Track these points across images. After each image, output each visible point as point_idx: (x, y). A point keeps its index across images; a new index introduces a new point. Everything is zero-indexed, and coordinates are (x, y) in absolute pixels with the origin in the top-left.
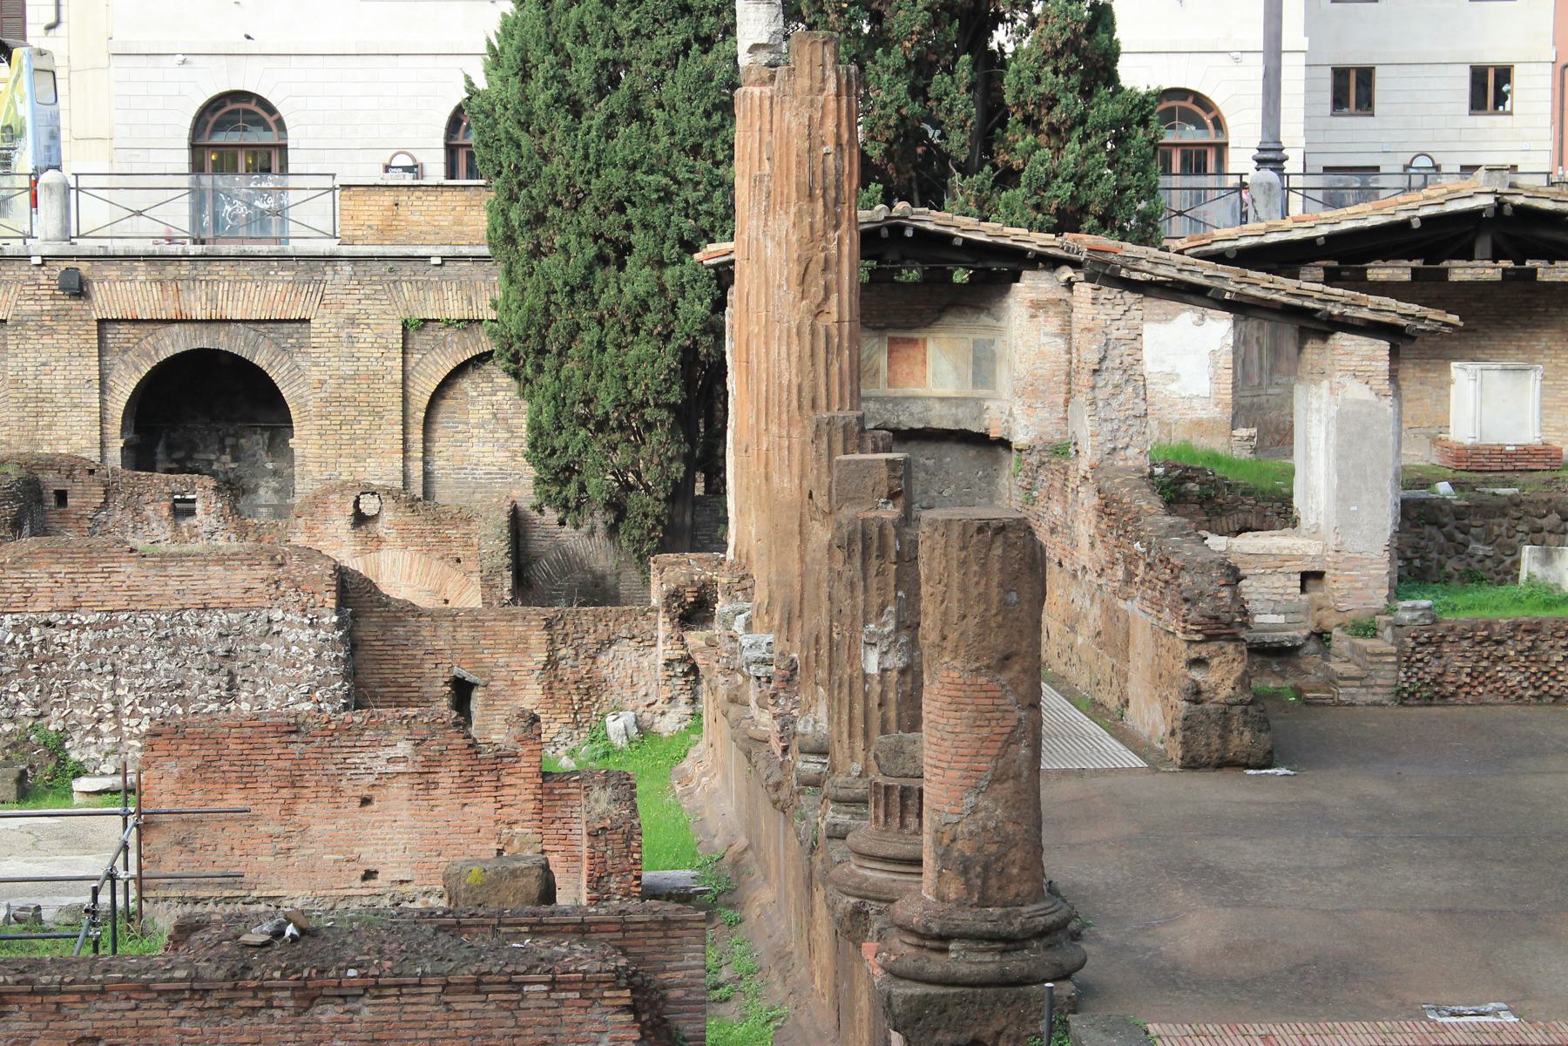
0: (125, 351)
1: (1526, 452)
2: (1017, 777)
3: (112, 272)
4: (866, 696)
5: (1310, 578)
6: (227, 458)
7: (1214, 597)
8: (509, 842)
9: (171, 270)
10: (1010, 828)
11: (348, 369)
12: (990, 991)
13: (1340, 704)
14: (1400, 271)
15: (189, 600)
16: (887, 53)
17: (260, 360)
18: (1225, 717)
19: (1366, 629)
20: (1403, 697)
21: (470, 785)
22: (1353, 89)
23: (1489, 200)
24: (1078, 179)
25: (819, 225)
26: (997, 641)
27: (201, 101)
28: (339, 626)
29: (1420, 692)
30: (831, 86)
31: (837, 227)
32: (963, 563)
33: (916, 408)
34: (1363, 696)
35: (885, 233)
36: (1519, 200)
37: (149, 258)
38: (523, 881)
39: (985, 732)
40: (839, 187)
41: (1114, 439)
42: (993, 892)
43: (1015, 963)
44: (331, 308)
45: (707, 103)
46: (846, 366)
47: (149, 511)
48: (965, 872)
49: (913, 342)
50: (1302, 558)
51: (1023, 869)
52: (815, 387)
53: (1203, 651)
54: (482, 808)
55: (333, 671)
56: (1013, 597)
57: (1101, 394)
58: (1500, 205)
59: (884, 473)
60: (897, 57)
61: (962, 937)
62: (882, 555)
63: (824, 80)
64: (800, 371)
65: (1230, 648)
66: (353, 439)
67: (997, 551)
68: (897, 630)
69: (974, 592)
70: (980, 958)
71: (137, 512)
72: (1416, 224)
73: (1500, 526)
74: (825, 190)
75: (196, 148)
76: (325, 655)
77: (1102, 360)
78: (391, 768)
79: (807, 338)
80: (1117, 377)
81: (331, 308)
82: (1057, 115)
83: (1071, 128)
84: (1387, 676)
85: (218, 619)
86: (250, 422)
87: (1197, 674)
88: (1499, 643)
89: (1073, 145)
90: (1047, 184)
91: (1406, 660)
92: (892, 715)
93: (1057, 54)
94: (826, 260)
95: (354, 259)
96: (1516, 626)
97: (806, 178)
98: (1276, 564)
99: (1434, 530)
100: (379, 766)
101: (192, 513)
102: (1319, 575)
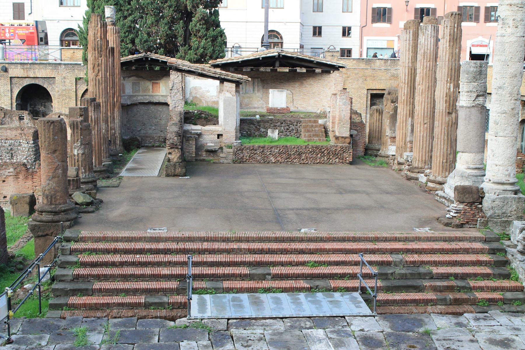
0: (16, 84)
1: (283, 109)
2: (58, 177)
3: (13, 67)
4: (75, 159)
5: (219, 136)
6: (43, 107)
7: (173, 139)
8: (35, 190)
9: (25, 66)
10: (57, 188)
11: (64, 88)
12: (50, 224)
13: (221, 163)
14: (248, 69)
15: (3, 138)
16: (163, 20)
17: (45, 86)
18: (175, 165)
19: (230, 147)
20: (234, 162)
21: (26, 178)
22: (317, 31)
23: (277, 54)
24: (204, 48)
25: (97, 56)
26: (53, 147)
27: (62, 30)
28: (33, 143)
29: (239, 160)
30: (99, 26)
31: (101, 57)
32: (44, 130)
33: (157, 98)
34: (226, 161)
35: (144, 59)
36: (283, 54)
37: (21, 64)
38: (25, 199)
39: (50, 167)
40: (101, 48)
41: (175, 104)
42: (53, 202)
43: (56, 218)
44: (59, 75)
45: (125, 30)
46: (103, 88)
47: (14, 118)
48: (47, 198)
49: (157, 83)
50: (217, 131)
51: (61, 197)
52: (96, 92)
53: (171, 151)
54: (29, 183)
55: (32, 153)
56: (56, 137)
57: (172, 95)
58: (279, 55)
59: (79, 110)
60: (166, 20)
61: (45, 212)
62: (77, 129)
63: (97, 24)
64: (93, 88)
65: (176, 150)
66: (65, 104)
67: (52, 127)
68: (81, 145)
69: (47, 136)
70: (49, 216)
71: (11, 119)
72: (261, 59)
73: (267, 125)
74: (98, 49)
75: (62, 41)
76: (30, 150)
77: (173, 87)
78: (9, 174)
79: (94, 81)
80: (176, 91)
81: (59, 75)
82: (200, 34)
83: (204, 37)
84: (231, 157)
85: (9, 142)
86: (48, 99)
87: (170, 156)
88: (255, 150)
89: (204, 41)
90: (198, 49)
91: (235, 154)
92: (80, 164)
93: (200, 21)
94: (98, 64)
95: (65, 64)
96: (259, 147)
97: (93, 46)
98: (212, 132)
99: (253, 126)
100: (7, 174)
101: (23, 119)
102: (222, 135)
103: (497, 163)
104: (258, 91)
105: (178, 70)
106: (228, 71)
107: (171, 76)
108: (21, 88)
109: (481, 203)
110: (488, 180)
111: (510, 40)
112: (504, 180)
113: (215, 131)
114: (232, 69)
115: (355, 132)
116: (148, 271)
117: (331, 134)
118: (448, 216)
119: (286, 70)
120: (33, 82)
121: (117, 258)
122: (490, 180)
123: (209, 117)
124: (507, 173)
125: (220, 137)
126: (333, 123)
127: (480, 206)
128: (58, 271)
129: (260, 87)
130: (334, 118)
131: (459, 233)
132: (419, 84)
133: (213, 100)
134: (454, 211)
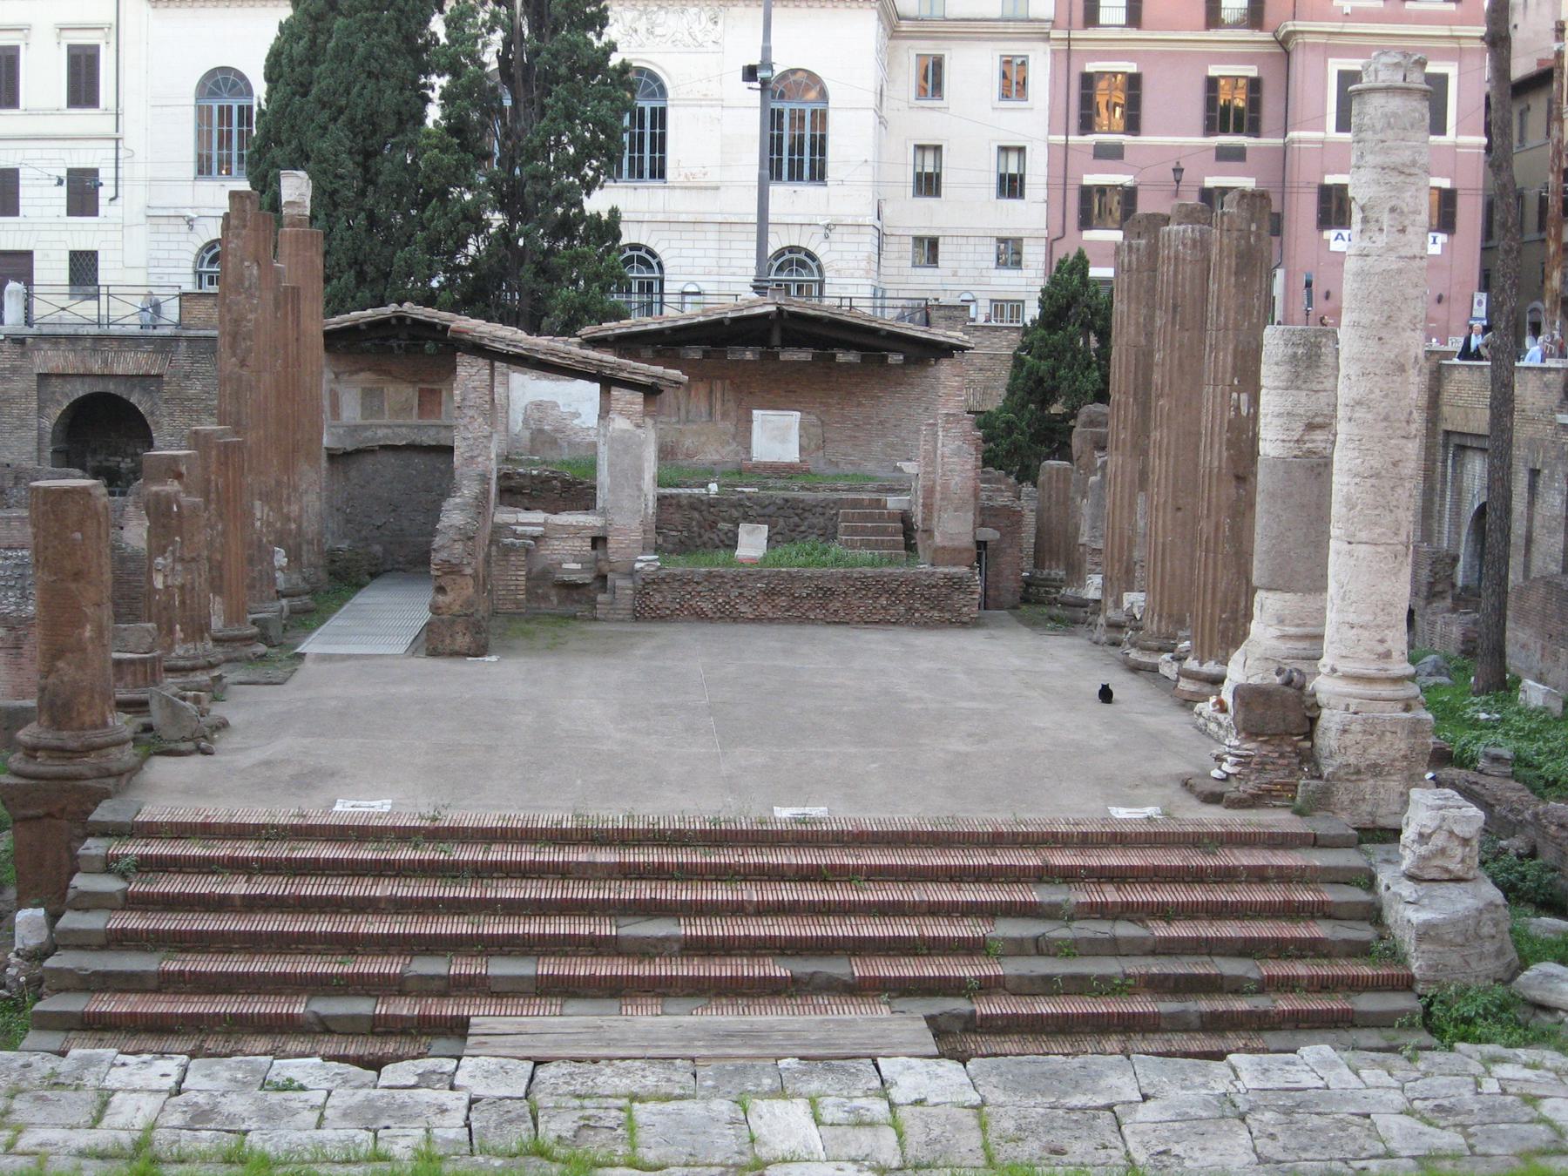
5: (598, 542)
23: (774, 308)
36: (792, 309)
58: (780, 311)
98: (576, 531)
103: (1352, 618)
104: (725, 415)
105: (478, 349)
106: (637, 358)
107: (459, 369)
108: (66, 404)
109: (1309, 735)
110: (1328, 669)
111: (1384, 266)
112: (1371, 669)
113: (585, 528)
114: (648, 353)
115: (989, 534)
116: (323, 925)
117: (919, 537)
118: (1216, 773)
119: (804, 355)
120: (99, 387)
121: (239, 887)
122: (1334, 670)
123: (571, 489)
124: (1381, 649)
125: (600, 543)
126: (924, 505)
127: (1308, 744)
128: (70, 920)
129: (731, 405)
130: (929, 492)
131: (1238, 820)
132: (1162, 395)
133: (588, 439)
134: (1230, 759)
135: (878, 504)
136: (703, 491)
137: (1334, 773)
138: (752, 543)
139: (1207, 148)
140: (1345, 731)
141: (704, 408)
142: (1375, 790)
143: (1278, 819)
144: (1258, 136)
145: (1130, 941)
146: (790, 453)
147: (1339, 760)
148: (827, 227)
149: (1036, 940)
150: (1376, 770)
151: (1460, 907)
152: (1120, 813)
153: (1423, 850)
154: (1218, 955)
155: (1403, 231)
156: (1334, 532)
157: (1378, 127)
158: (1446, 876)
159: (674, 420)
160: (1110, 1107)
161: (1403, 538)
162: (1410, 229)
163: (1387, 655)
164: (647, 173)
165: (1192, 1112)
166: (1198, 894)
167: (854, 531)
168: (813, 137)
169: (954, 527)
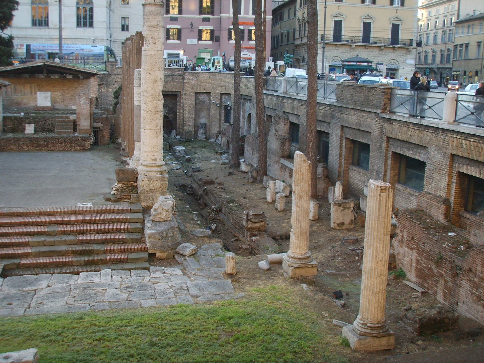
23: (42, 64)
36: (48, 64)
58: (45, 64)
103: (146, 150)
109: (136, 182)
111: (150, 53)
117: (78, 128)
118: (112, 193)
122: (142, 164)
124: (153, 158)
127: (136, 184)
135: (68, 117)
136: (19, 115)
137: (140, 192)
138: (30, 129)
139: (200, 18)
140: (143, 181)
141: (29, 91)
142: (152, 196)
143: (124, 206)
144: (213, 15)
145: (70, 241)
146: (48, 104)
147: (142, 188)
148: (94, 40)
149: (43, 241)
150: (152, 191)
151: (163, 228)
152: (80, 205)
153: (155, 213)
154: (96, 244)
155: (155, 43)
156: (141, 126)
157: (148, 15)
158: (162, 220)
159: (20, 94)
160: (35, 290)
161: (159, 127)
162: (157, 43)
163: (155, 160)
164: (37, 24)
165: (57, 290)
166: (93, 227)
167: (59, 125)
168: (90, 15)
169: (85, 124)
